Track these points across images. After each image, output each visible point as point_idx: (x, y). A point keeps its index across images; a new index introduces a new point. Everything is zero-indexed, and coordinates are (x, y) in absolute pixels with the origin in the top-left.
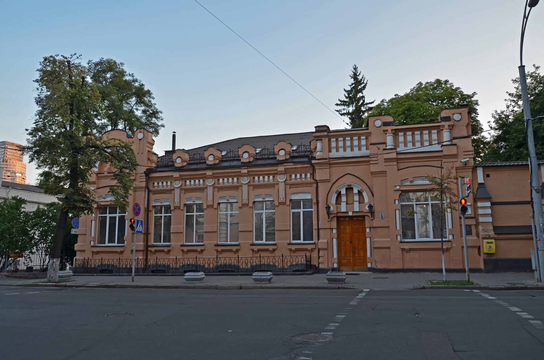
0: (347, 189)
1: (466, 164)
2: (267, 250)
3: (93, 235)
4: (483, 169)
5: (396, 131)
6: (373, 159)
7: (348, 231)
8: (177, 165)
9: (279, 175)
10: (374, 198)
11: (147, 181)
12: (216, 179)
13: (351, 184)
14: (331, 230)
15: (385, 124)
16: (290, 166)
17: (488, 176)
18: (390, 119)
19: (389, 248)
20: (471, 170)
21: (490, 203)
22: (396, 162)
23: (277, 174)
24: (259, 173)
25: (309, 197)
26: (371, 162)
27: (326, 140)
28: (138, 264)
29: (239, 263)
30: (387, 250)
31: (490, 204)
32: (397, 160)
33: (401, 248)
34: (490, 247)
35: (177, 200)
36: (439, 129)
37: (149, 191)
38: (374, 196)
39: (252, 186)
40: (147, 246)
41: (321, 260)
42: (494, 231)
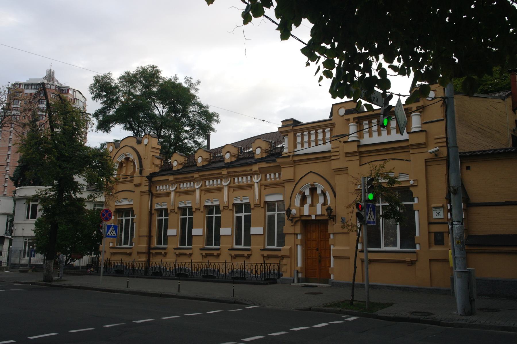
1: (436, 155)
7: (314, 237)
9: (255, 175)
10: (336, 198)
11: (150, 187)
13: (314, 184)
14: (296, 236)
16: (263, 165)
24: (237, 174)
26: (332, 158)
27: (291, 135)
32: (360, 154)
33: (361, 259)
37: (152, 195)
39: (231, 188)
40: (150, 248)
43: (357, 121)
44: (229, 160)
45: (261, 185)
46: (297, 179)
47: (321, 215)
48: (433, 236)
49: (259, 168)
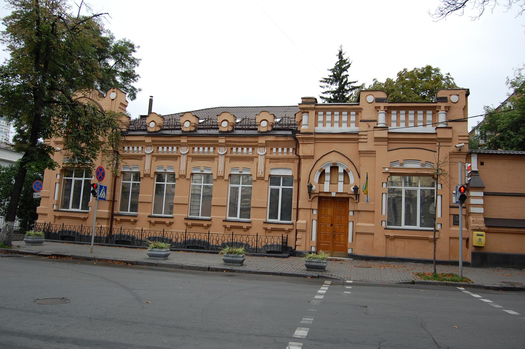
0: (332, 168)
1: (460, 150)
2: (241, 228)
3: (56, 198)
4: (477, 157)
5: (389, 108)
6: (362, 137)
7: (329, 213)
8: (150, 130)
12: (191, 148)
14: (312, 210)
15: (378, 100)
17: (482, 164)
18: (383, 95)
19: (373, 234)
20: (465, 156)
21: (483, 192)
22: (387, 142)
23: (257, 146)
24: (237, 144)
25: (289, 173)
26: (360, 140)
27: (312, 113)
28: (101, 233)
29: (210, 240)
30: (371, 236)
31: (483, 194)
32: (388, 140)
34: (480, 240)
35: (147, 167)
36: (435, 110)
38: (361, 177)
39: (229, 157)
40: (112, 215)
41: (298, 242)
42: (485, 223)
43: (387, 109)
44: (227, 128)
45: (266, 158)
46: (317, 157)
47: (328, 192)
48: (452, 217)
49: (266, 141)
